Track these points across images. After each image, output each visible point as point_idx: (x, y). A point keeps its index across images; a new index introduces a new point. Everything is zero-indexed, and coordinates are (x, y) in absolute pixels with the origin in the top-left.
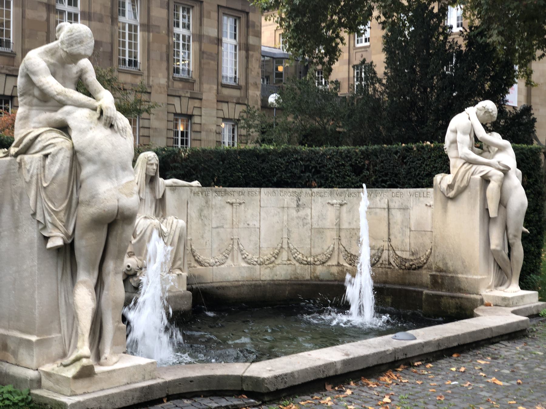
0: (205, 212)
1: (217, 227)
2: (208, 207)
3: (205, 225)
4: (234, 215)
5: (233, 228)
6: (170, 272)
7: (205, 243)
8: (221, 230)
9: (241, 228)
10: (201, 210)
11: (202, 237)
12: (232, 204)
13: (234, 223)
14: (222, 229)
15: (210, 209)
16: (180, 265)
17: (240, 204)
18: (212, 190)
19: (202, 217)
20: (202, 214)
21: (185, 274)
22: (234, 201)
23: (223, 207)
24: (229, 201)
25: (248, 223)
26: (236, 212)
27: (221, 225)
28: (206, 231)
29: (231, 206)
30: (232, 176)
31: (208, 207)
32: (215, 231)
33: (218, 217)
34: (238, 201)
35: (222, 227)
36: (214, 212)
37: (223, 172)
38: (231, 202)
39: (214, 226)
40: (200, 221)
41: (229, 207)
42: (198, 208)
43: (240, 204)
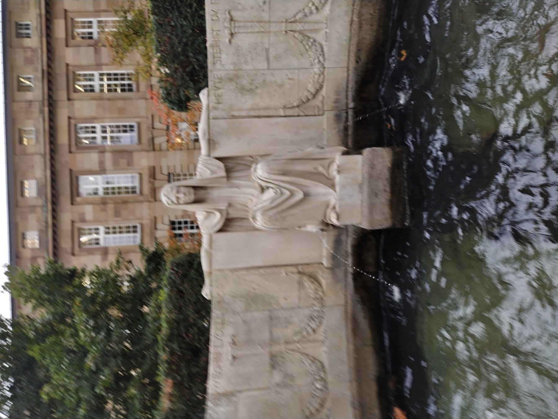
0: (245, 82)
1: (268, 60)
2: (238, 77)
3: (264, 81)
4: (250, 30)
5: (269, 32)
6: (333, 186)
7: (291, 82)
8: (272, 53)
9: (270, 16)
10: (243, 90)
11: (281, 86)
12: (232, 34)
13: (262, 30)
14: (271, 51)
15: (241, 73)
16: (323, 166)
17: (232, 20)
18: (211, 71)
19: (253, 87)
20: (248, 87)
21: (339, 159)
22: (227, 32)
23: (238, 51)
24: (227, 41)
25: (261, 4)
26: (245, 27)
27: (264, 53)
28: (273, 79)
29: (235, 36)
30: (190, 6)
31: (238, 77)
32: (274, 65)
33: (252, 59)
34: (227, 25)
35: (267, 50)
36: (244, 67)
37: (186, 18)
38: (229, 36)
39: (264, 65)
40: (259, 91)
41: (237, 40)
42: (240, 94)
43: (232, 20)
